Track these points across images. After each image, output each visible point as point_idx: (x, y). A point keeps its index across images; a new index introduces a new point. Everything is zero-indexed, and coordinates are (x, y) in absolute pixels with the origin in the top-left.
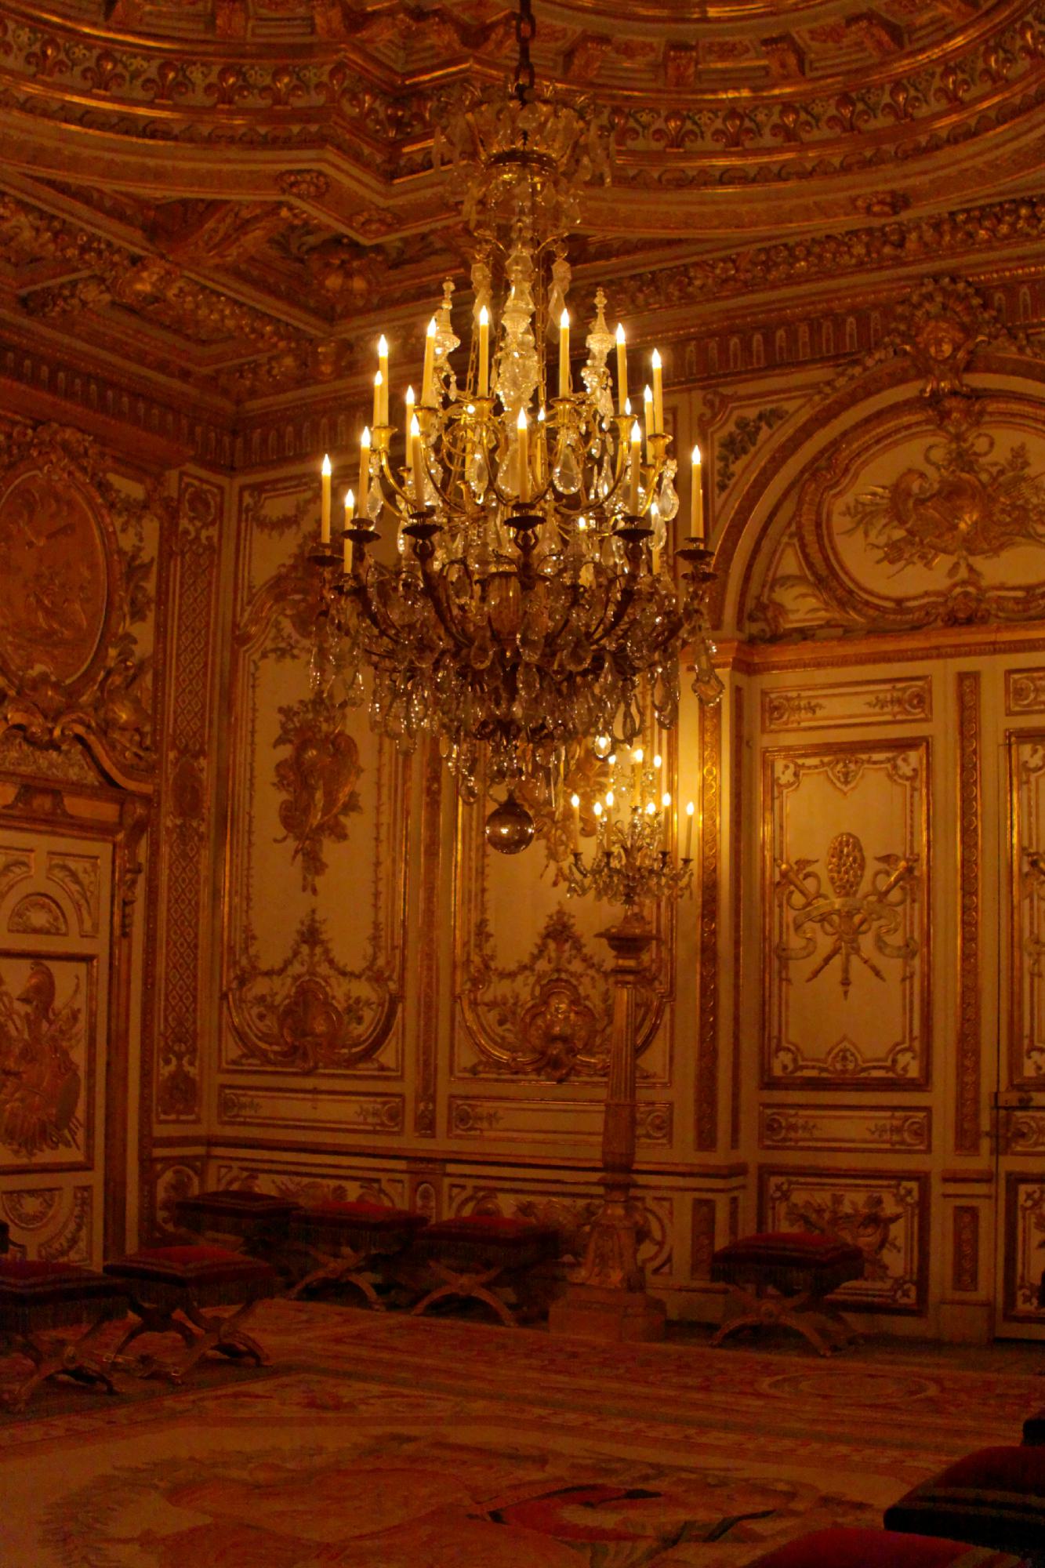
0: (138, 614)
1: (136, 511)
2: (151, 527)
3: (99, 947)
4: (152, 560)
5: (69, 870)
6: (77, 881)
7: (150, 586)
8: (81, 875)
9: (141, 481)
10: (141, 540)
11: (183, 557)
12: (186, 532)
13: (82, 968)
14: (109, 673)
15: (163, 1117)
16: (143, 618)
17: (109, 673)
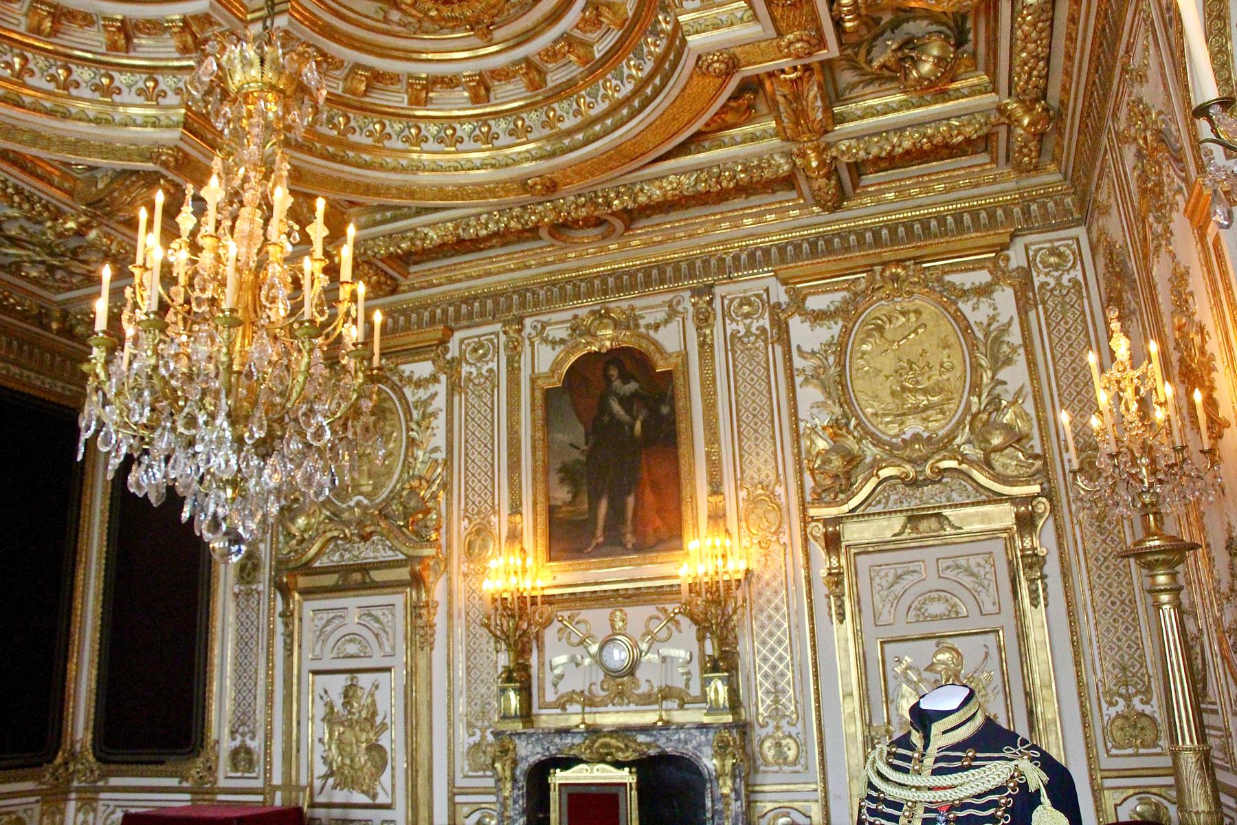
0: (1000, 361)
1: (984, 291)
2: (1005, 299)
3: (1006, 620)
4: (1012, 318)
5: (958, 567)
6: (972, 574)
7: (1015, 336)
8: (975, 570)
9: (982, 268)
10: (995, 309)
11: (1044, 303)
12: (1043, 285)
13: (992, 637)
14: (974, 416)
15: (1114, 751)
16: (1008, 361)
17: (974, 416)
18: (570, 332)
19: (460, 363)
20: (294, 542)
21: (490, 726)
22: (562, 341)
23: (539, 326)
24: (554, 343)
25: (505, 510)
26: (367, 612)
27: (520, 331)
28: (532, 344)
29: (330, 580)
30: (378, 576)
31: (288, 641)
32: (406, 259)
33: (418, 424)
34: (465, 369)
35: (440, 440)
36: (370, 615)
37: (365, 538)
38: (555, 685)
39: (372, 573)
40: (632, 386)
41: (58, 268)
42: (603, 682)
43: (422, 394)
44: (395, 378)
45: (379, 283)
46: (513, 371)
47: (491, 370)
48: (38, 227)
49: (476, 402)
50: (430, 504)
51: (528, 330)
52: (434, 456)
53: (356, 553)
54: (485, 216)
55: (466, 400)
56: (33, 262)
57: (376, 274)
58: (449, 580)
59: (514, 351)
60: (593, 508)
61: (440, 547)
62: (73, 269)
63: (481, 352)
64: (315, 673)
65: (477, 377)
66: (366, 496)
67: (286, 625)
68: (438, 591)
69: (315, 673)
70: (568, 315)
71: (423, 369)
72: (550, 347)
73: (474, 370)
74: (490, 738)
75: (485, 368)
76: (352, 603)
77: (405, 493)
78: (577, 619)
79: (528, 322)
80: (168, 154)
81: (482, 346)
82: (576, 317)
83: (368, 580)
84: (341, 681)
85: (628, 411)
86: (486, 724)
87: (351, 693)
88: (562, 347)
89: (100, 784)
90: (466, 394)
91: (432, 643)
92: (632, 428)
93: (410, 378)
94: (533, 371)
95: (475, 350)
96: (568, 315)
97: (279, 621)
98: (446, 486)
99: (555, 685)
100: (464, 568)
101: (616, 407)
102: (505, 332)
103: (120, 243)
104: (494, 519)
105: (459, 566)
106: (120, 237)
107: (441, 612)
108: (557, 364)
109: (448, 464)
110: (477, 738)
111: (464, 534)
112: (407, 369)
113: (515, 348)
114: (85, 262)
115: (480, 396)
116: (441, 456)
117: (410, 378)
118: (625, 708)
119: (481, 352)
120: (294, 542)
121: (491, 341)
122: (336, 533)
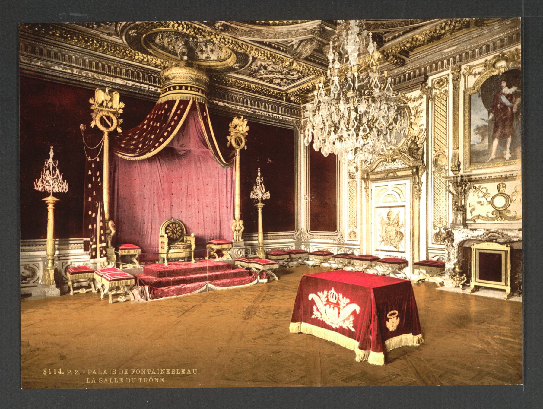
18: (483, 68)
19: (431, 89)
20: (368, 164)
21: (443, 226)
22: (479, 73)
23: (468, 68)
24: (475, 75)
25: (451, 146)
26: (396, 186)
27: (460, 71)
28: (465, 76)
29: (383, 175)
30: (399, 174)
31: (367, 197)
32: (405, 53)
33: (415, 116)
34: (434, 91)
35: (423, 121)
36: (396, 187)
37: (394, 160)
38: (471, 212)
39: (397, 173)
40: (514, 89)
41: (284, 78)
42: (493, 212)
43: (416, 104)
44: (404, 100)
45: (397, 62)
46: (456, 88)
47: (446, 91)
48: (277, 66)
49: (439, 104)
50: (419, 146)
51: (463, 71)
52: (421, 128)
53: (390, 166)
54: (444, 24)
55: (435, 104)
56: (276, 78)
57: (396, 59)
58: (427, 173)
59: (456, 80)
60: (490, 144)
61: (423, 162)
62: (288, 78)
63: (441, 83)
64: (377, 207)
65: (439, 94)
66: (394, 145)
67: (366, 192)
68: (423, 179)
69: (377, 207)
70: (482, 60)
71: (416, 93)
72: (473, 77)
73: (438, 92)
74: (443, 231)
75: (443, 89)
76: (390, 184)
77: (409, 143)
78: (481, 188)
79: (463, 67)
80: (317, 30)
81: (441, 80)
82: (486, 61)
83: (396, 175)
84: (388, 210)
85: (510, 101)
86: (441, 226)
87: (390, 214)
88: (479, 75)
89: (310, 241)
90: (435, 101)
91: (420, 197)
92: (512, 108)
93: (411, 99)
94: (465, 88)
95: (438, 83)
96: (482, 60)
97: (364, 191)
98: (427, 139)
99: (471, 212)
100: (433, 170)
101: (504, 99)
102: (452, 74)
103: (303, 67)
104: (446, 150)
105: (432, 169)
106: (303, 64)
107: (424, 185)
108: (477, 83)
109: (427, 130)
110: (437, 231)
111: (433, 156)
112: (408, 95)
113: (457, 79)
114: (293, 75)
115: (440, 102)
116: (424, 127)
117: (411, 99)
118: (502, 222)
119: (441, 83)
120: (368, 164)
121: (446, 78)
122: (383, 159)
